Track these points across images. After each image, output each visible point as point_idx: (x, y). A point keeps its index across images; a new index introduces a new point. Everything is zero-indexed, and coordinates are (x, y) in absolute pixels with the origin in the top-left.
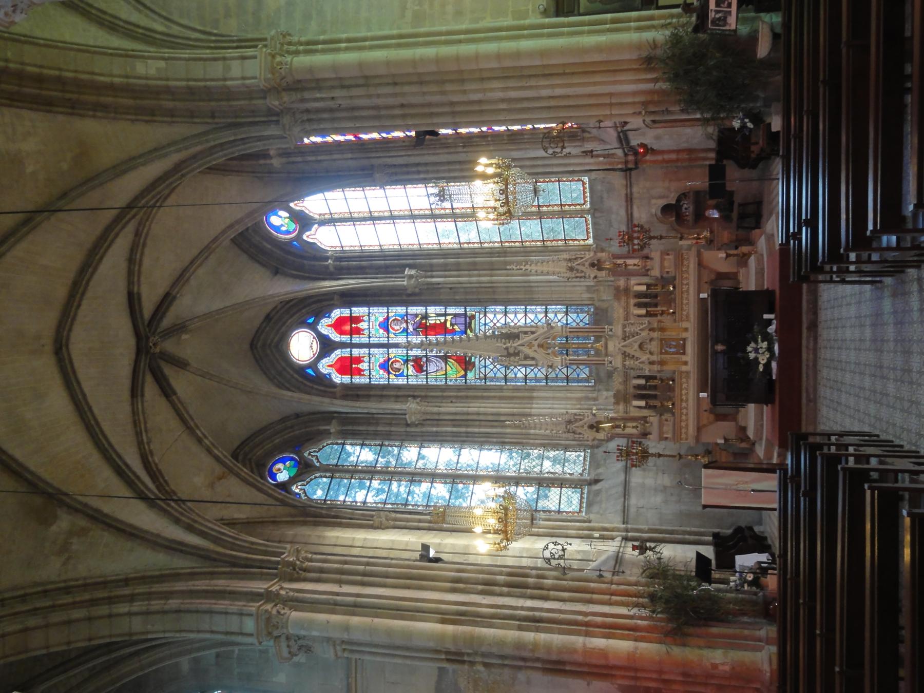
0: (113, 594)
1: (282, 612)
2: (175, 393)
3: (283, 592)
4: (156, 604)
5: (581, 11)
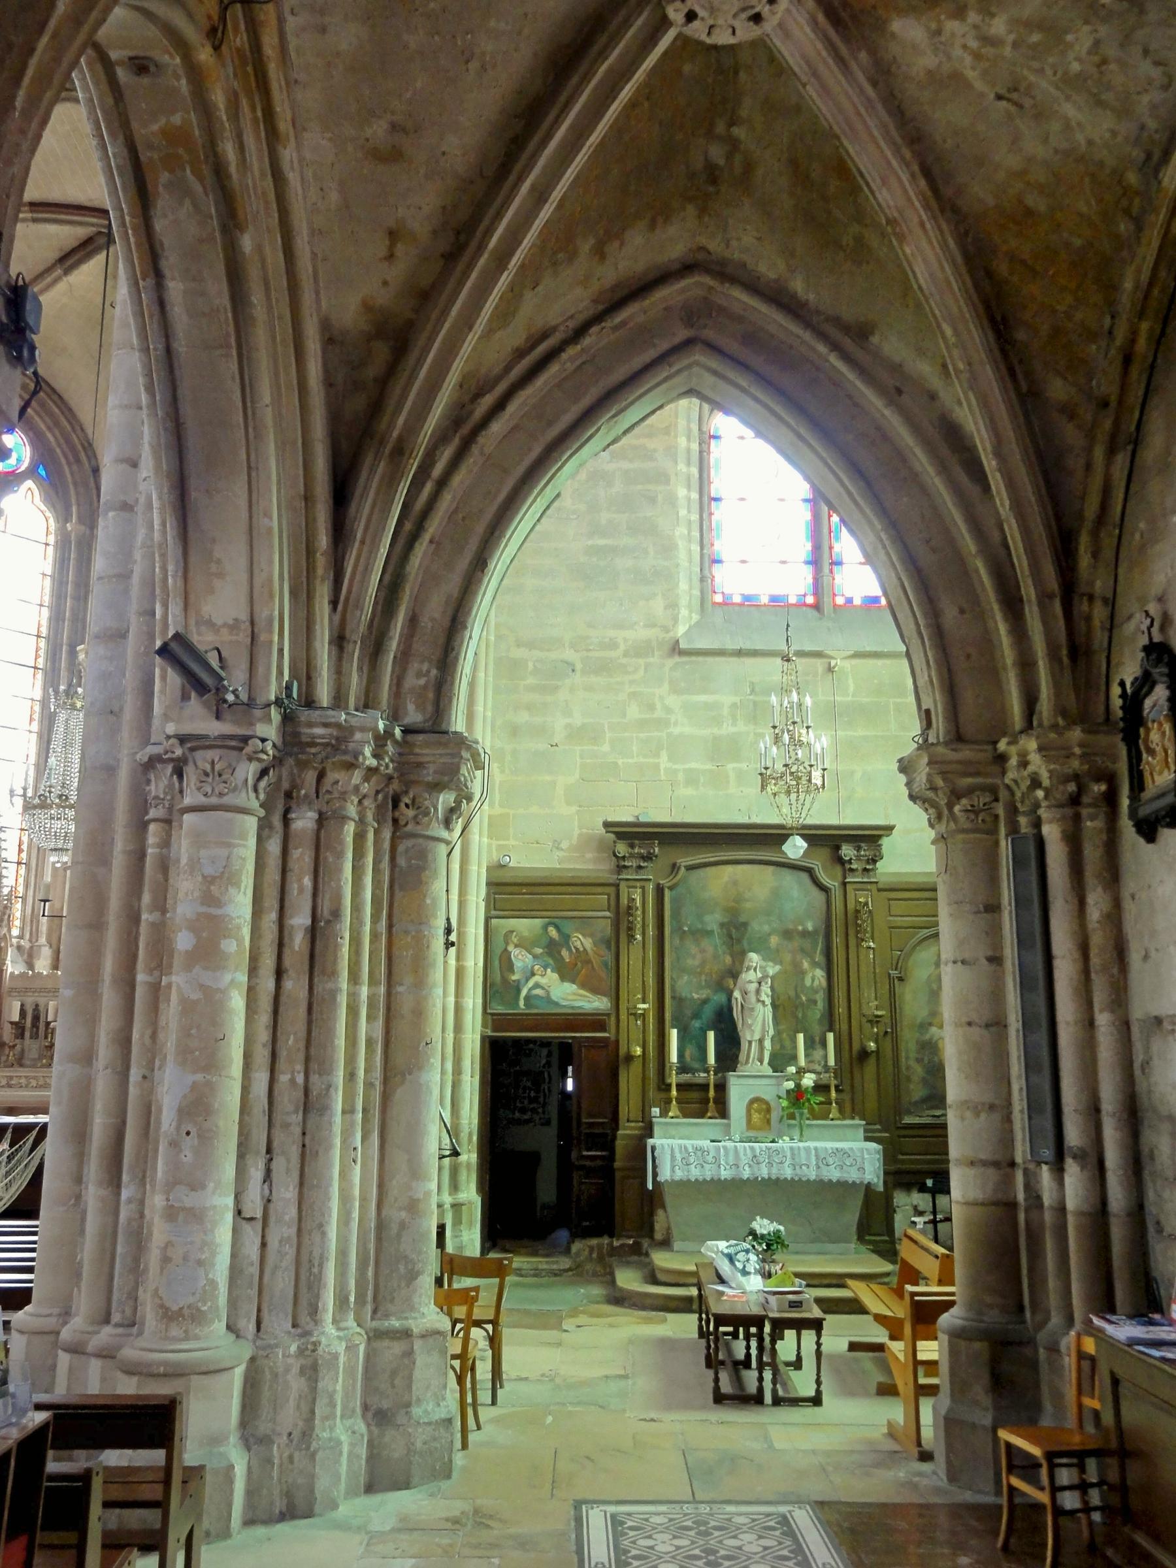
2: (67, 272)
5: (494, 921)
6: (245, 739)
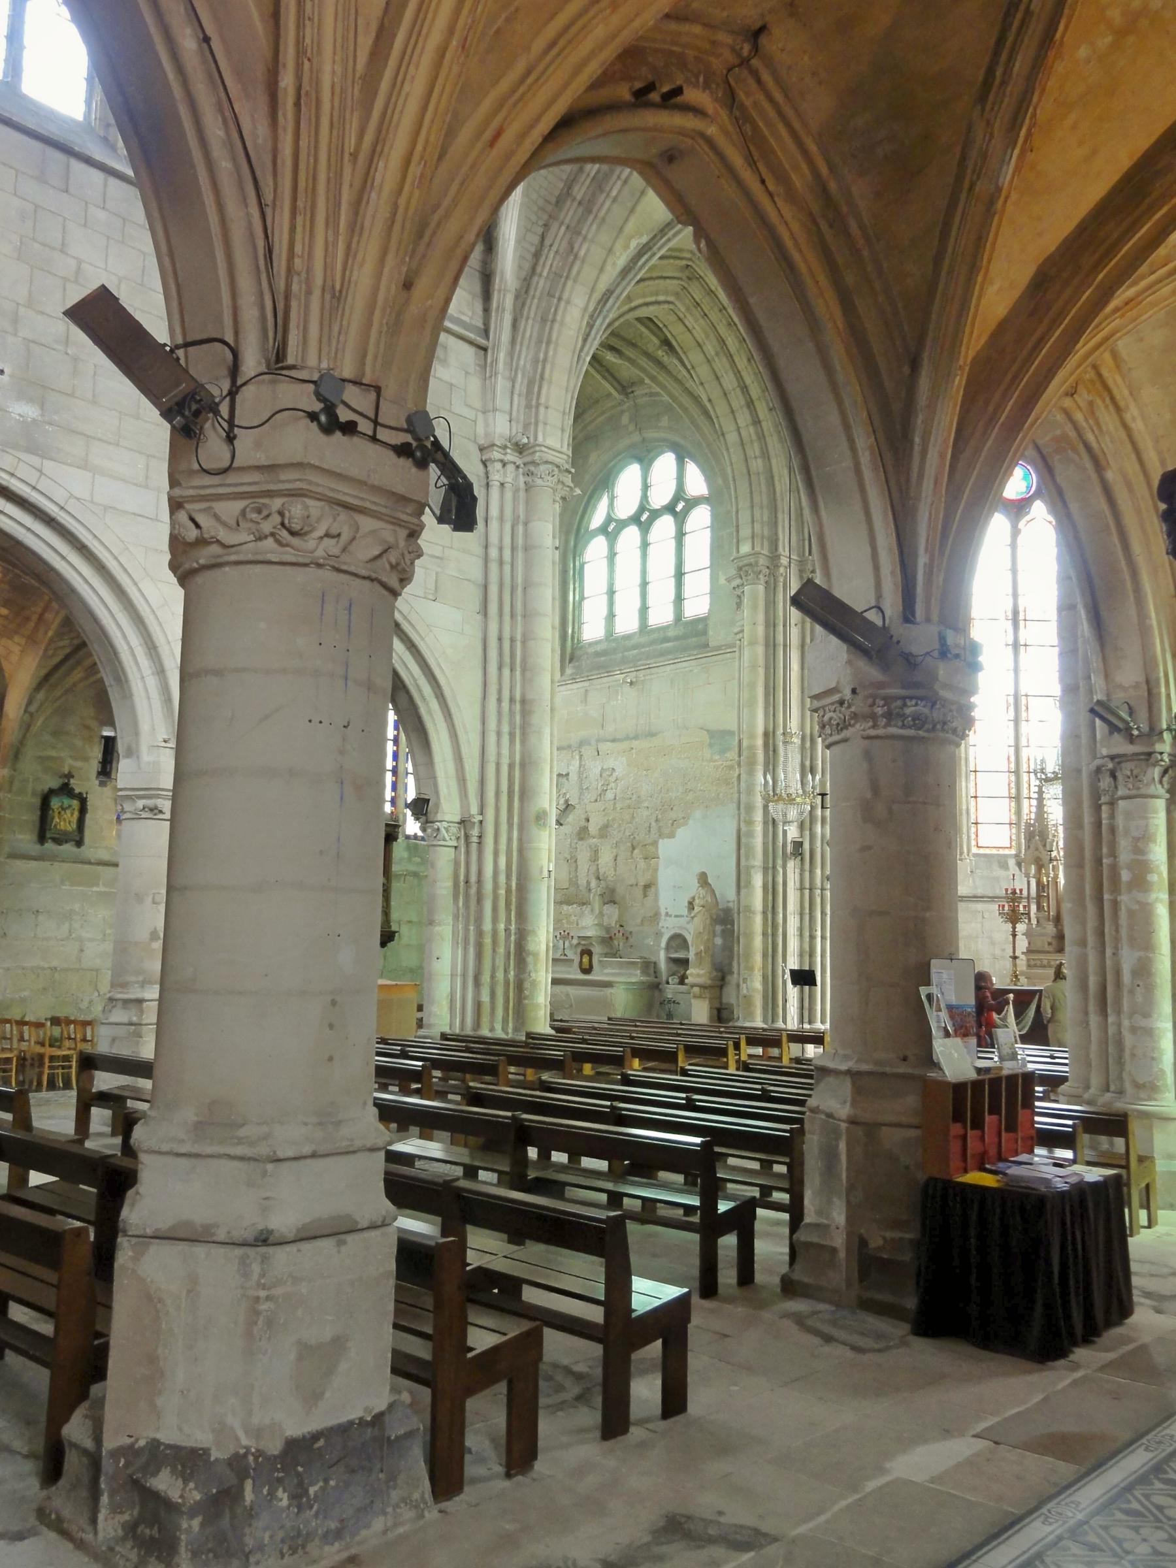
0: (757, 404)
1: (761, 576)
3: (782, 570)
4: (754, 450)
6: (1150, 754)
